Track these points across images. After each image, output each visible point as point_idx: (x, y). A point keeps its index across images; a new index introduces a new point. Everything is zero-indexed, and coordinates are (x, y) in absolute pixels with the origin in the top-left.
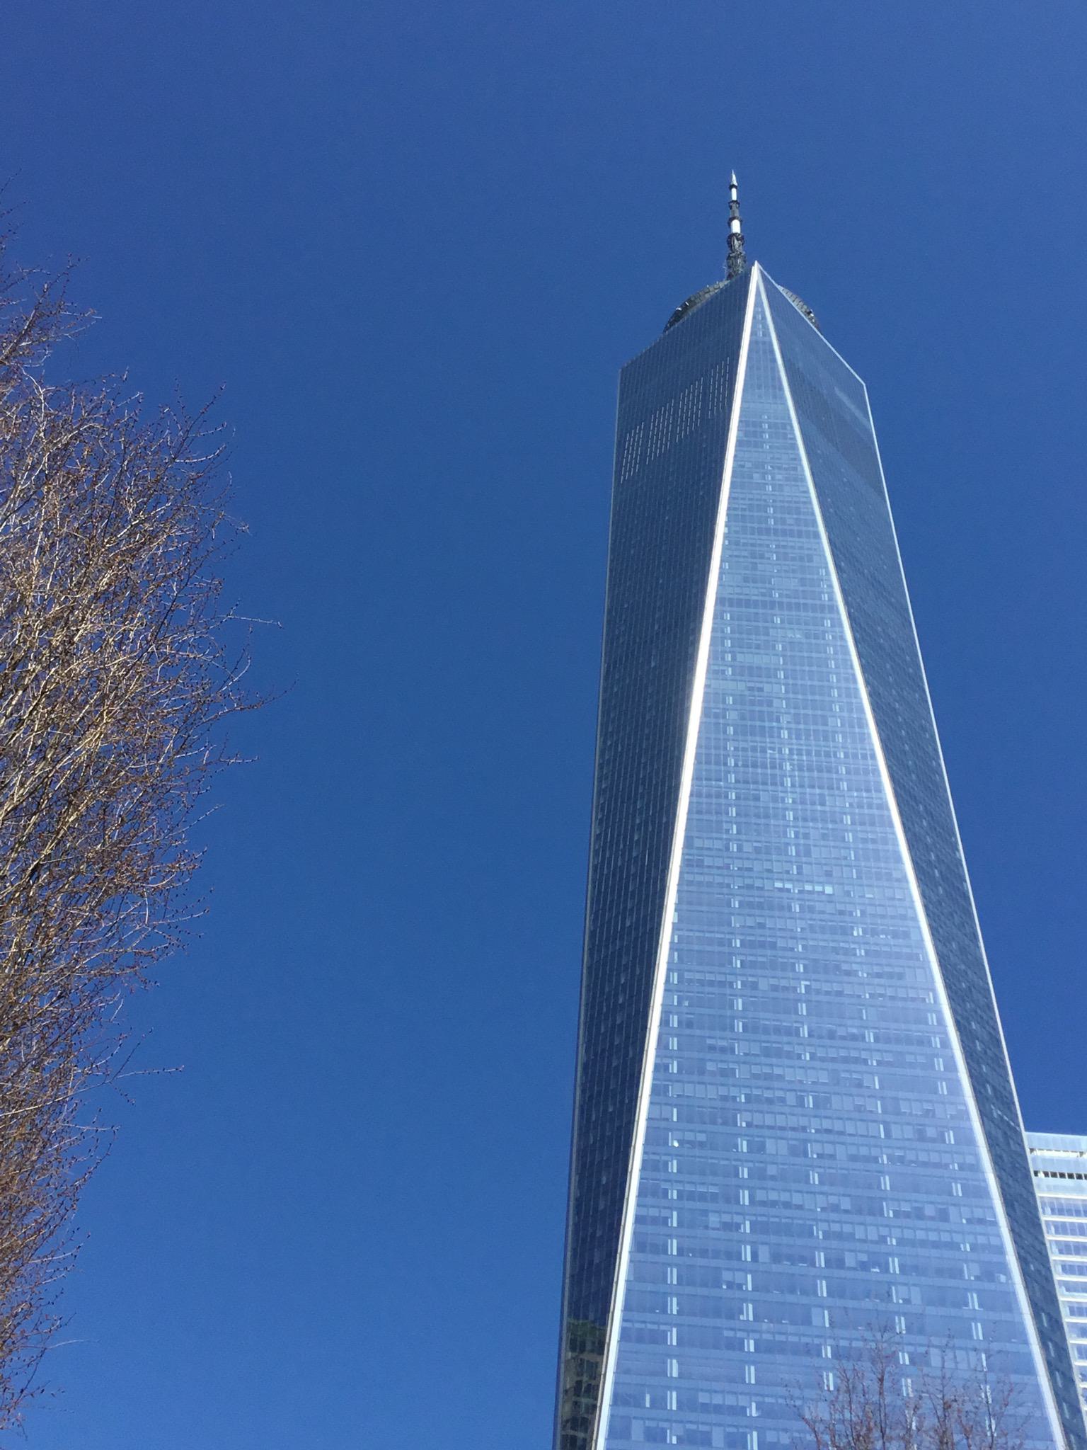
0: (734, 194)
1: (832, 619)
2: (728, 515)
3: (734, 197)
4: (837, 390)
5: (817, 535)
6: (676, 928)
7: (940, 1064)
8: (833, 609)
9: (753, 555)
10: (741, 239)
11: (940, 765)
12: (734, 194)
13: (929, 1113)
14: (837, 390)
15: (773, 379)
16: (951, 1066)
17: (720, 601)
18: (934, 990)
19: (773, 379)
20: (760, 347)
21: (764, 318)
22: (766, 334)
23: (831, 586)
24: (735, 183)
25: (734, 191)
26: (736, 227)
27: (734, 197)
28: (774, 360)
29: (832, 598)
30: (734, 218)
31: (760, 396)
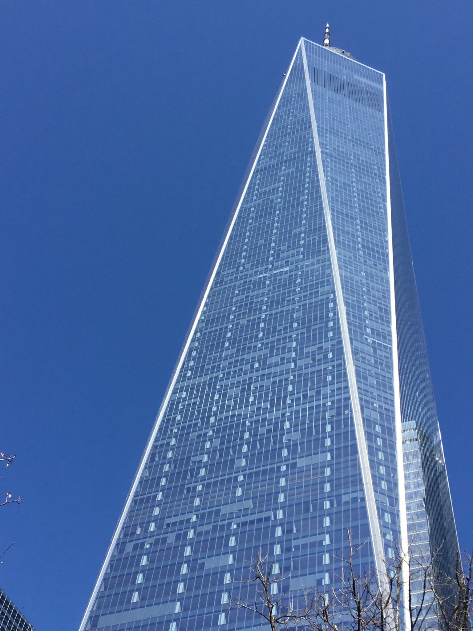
0: (327, 30)
1: (311, 157)
5: (310, 127)
6: (204, 313)
8: (313, 153)
9: (276, 147)
11: (385, 206)
12: (327, 30)
13: (320, 348)
14: (356, 77)
17: (256, 172)
21: (301, 55)
24: (328, 26)
30: (325, 39)
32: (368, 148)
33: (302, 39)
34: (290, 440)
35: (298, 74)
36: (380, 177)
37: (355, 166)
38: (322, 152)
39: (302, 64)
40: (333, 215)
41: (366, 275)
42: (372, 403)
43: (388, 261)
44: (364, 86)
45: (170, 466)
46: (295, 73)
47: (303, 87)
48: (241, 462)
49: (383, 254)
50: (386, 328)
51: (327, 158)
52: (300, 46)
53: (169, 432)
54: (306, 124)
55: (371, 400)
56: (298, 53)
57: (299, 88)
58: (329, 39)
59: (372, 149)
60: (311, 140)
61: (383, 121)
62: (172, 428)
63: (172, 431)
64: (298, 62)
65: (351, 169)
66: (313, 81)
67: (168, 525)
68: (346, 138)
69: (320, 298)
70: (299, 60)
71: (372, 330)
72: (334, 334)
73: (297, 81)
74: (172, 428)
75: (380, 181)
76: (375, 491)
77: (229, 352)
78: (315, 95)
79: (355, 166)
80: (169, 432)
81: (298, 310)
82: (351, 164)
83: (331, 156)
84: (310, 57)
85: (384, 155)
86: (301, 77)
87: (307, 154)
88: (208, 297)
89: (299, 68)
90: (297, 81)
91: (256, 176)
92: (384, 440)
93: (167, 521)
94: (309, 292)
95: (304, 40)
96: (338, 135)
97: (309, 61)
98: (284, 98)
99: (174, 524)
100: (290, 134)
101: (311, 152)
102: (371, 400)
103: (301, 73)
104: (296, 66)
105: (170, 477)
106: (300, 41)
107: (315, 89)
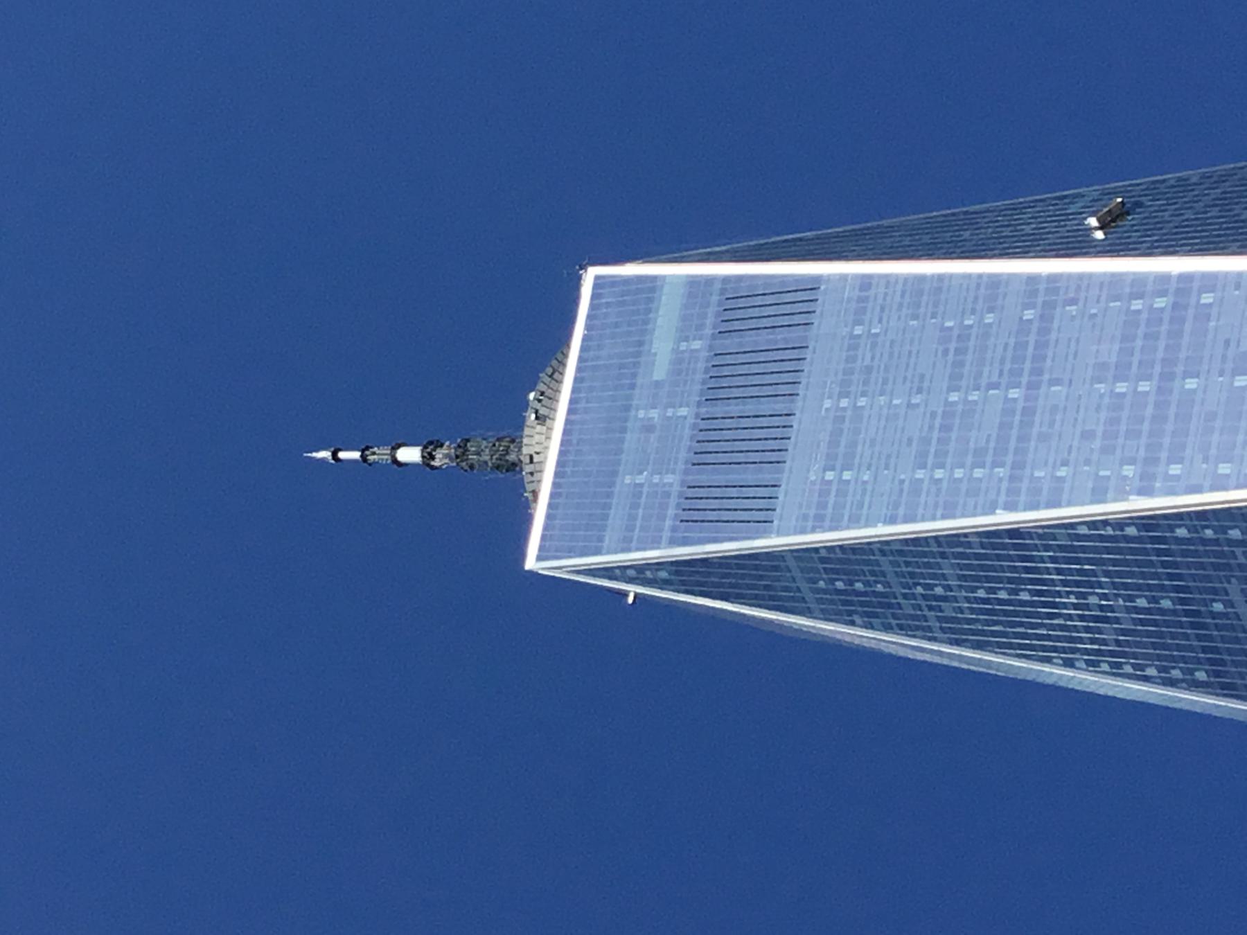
2: (1048, 660)
3: (356, 455)
4: (660, 371)
8: (1149, 523)
10: (429, 448)
15: (739, 567)
19: (739, 567)
22: (660, 566)
23: (1105, 523)
24: (325, 454)
25: (342, 455)
26: (410, 455)
27: (356, 455)
28: (704, 562)
30: (395, 461)
31: (786, 589)
33: (531, 563)
37: (1167, 377)
44: (697, 345)
47: (798, 559)
51: (1168, 478)
52: (578, 572)
56: (611, 578)
58: (395, 448)
64: (663, 574)
66: (764, 524)
70: (649, 574)
79: (1167, 377)
83: (1152, 461)
89: (688, 574)
95: (540, 558)
97: (655, 543)
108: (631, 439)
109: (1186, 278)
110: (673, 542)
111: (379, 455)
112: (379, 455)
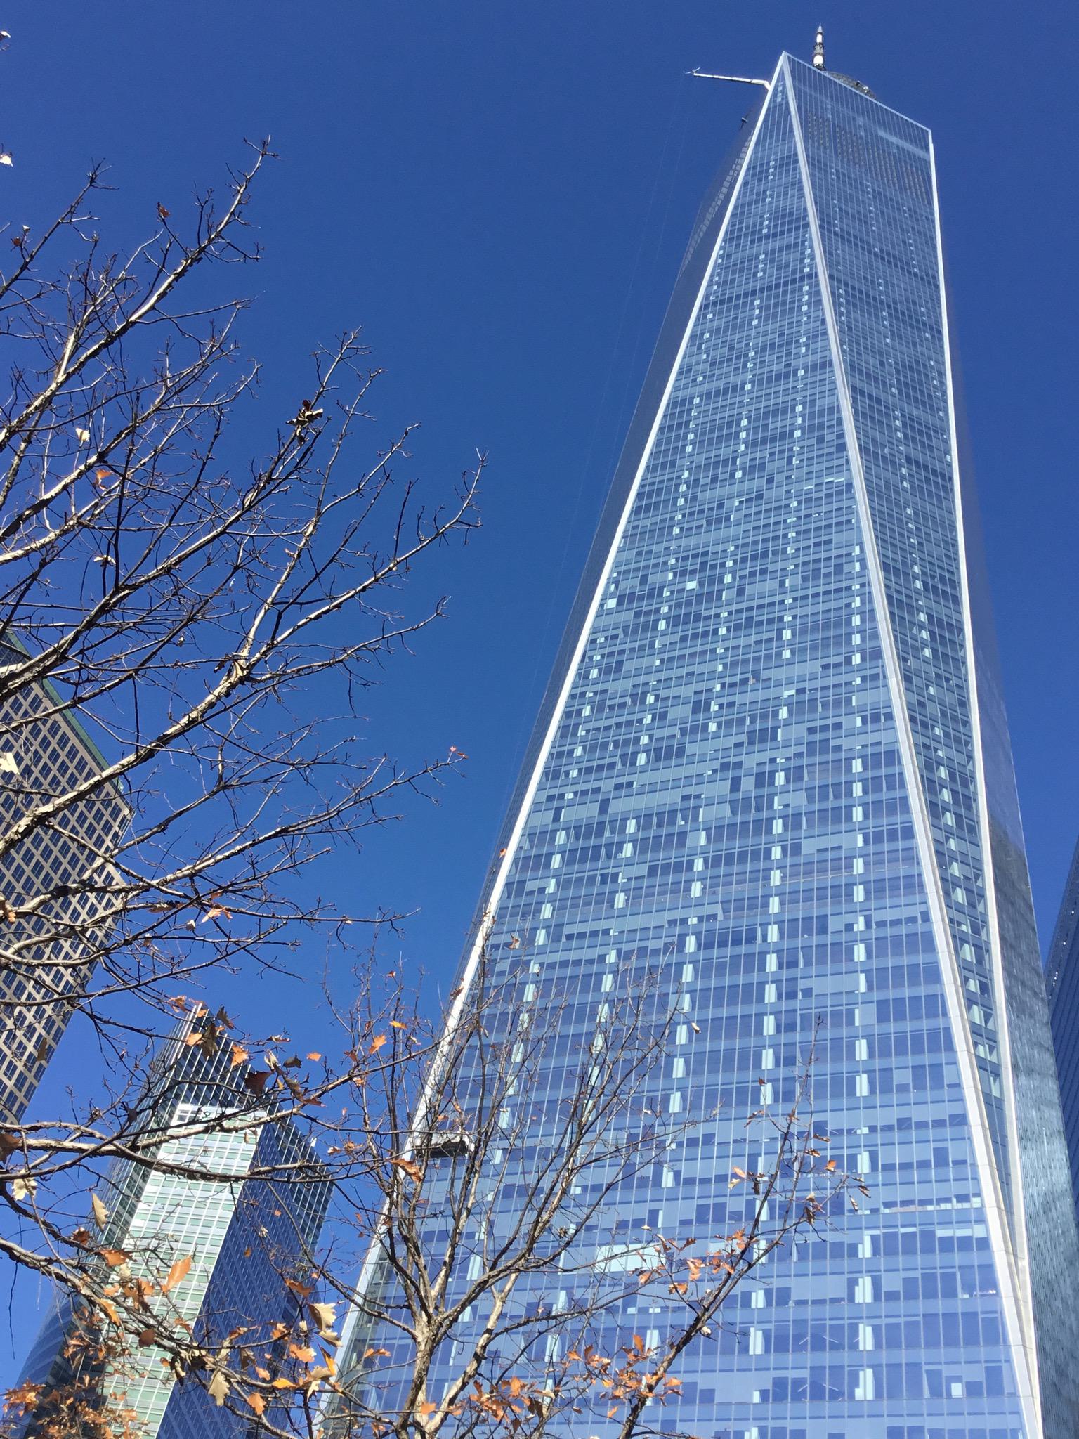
2: (724, 240)
4: (881, 133)
5: (807, 225)
7: (857, 602)
8: (813, 275)
11: (943, 384)
12: (819, 39)
14: (881, 133)
16: (867, 598)
17: (705, 307)
18: (861, 545)
19: (785, 127)
20: (780, 110)
21: (784, 86)
24: (820, 30)
29: (812, 266)
32: (909, 272)
34: (786, 806)
35: (779, 123)
36: (931, 328)
38: (831, 277)
39: (787, 103)
40: (855, 400)
41: (916, 514)
42: (936, 750)
43: (952, 490)
45: (568, 835)
46: (773, 120)
47: (790, 148)
48: (698, 839)
49: (943, 476)
50: (954, 615)
53: (563, 776)
54: (798, 220)
55: (933, 744)
57: (783, 151)
59: (915, 275)
60: (808, 251)
61: (933, 221)
62: (567, 768)
63: (567, 773)
64: (779, 100)
65: (882, 310)
67: (570, 937)
68: (869, 252)
69: (834, 553)
71: (930, 616)
72: (863, 620)
73: (778, 134)
74: (567, 768)
75: (933, 336)
76: (947, 906)
77: (668, 639)
78: (813, 165)
80: (563, 776)
81: (794, 573)
82: (882, 302)
83: (846, 284)
84: (800, 90)
85: (937, 287)
86: (785, 127)
87: (802, 279)
88: (624, 537)
89: (780, 110)
90: (778, 134)
91: (705, 316)
92: (958, 817)
93: (567, 930)
94: (813, 541)
96: (856, 245)
98: (755, 168)
99: (582, 936)
100: (767, 237)
101: (810, 276)
102: (933, 744)
103: (785, 121)
104: (775, 107)
105: (570, 857)
106: (781, 58)
107: (813, 153)
108: (848, 113)
109: (940, 333)
110: (799, 108)
111: (818, 49)
112: (818, 49)
